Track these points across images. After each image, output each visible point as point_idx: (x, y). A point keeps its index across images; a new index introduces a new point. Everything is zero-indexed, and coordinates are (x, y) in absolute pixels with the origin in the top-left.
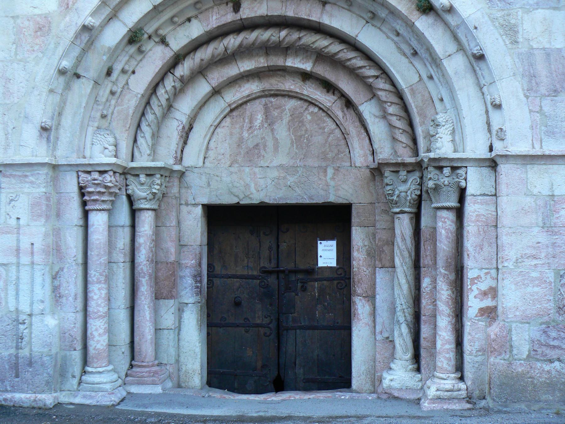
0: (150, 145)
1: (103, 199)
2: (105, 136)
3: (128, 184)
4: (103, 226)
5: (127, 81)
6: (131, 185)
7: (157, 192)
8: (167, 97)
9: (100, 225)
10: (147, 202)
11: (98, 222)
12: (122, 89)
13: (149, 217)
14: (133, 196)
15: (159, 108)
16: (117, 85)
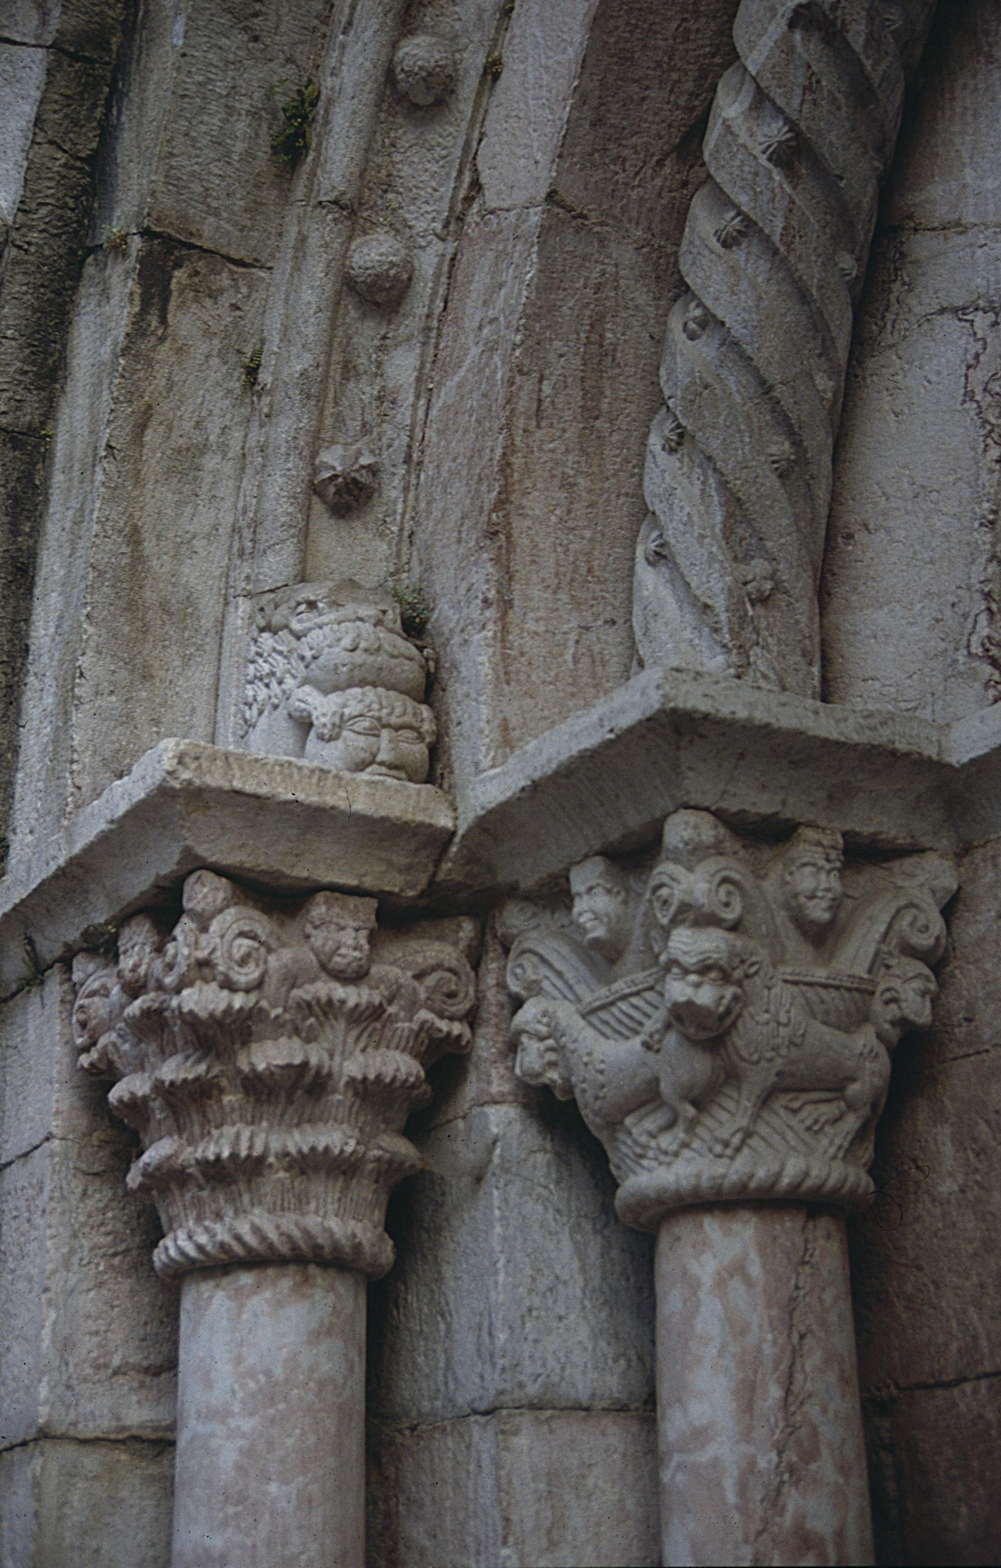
0: (720, 603)
1: (199, 1155)
2: (295, 626)
3: (515, 987)
4: (247, 1425)
5: (469, 158)
6: (534, 989)
7: (706, 996)
8: (775, 131)
9: (223, 1415)
10: (679, 1133)
11: (208, 1383)
12: (450, 247)
13: (720, 1284)
14: (569, 1088)
15: (739, 255)
16: (398, 228)
